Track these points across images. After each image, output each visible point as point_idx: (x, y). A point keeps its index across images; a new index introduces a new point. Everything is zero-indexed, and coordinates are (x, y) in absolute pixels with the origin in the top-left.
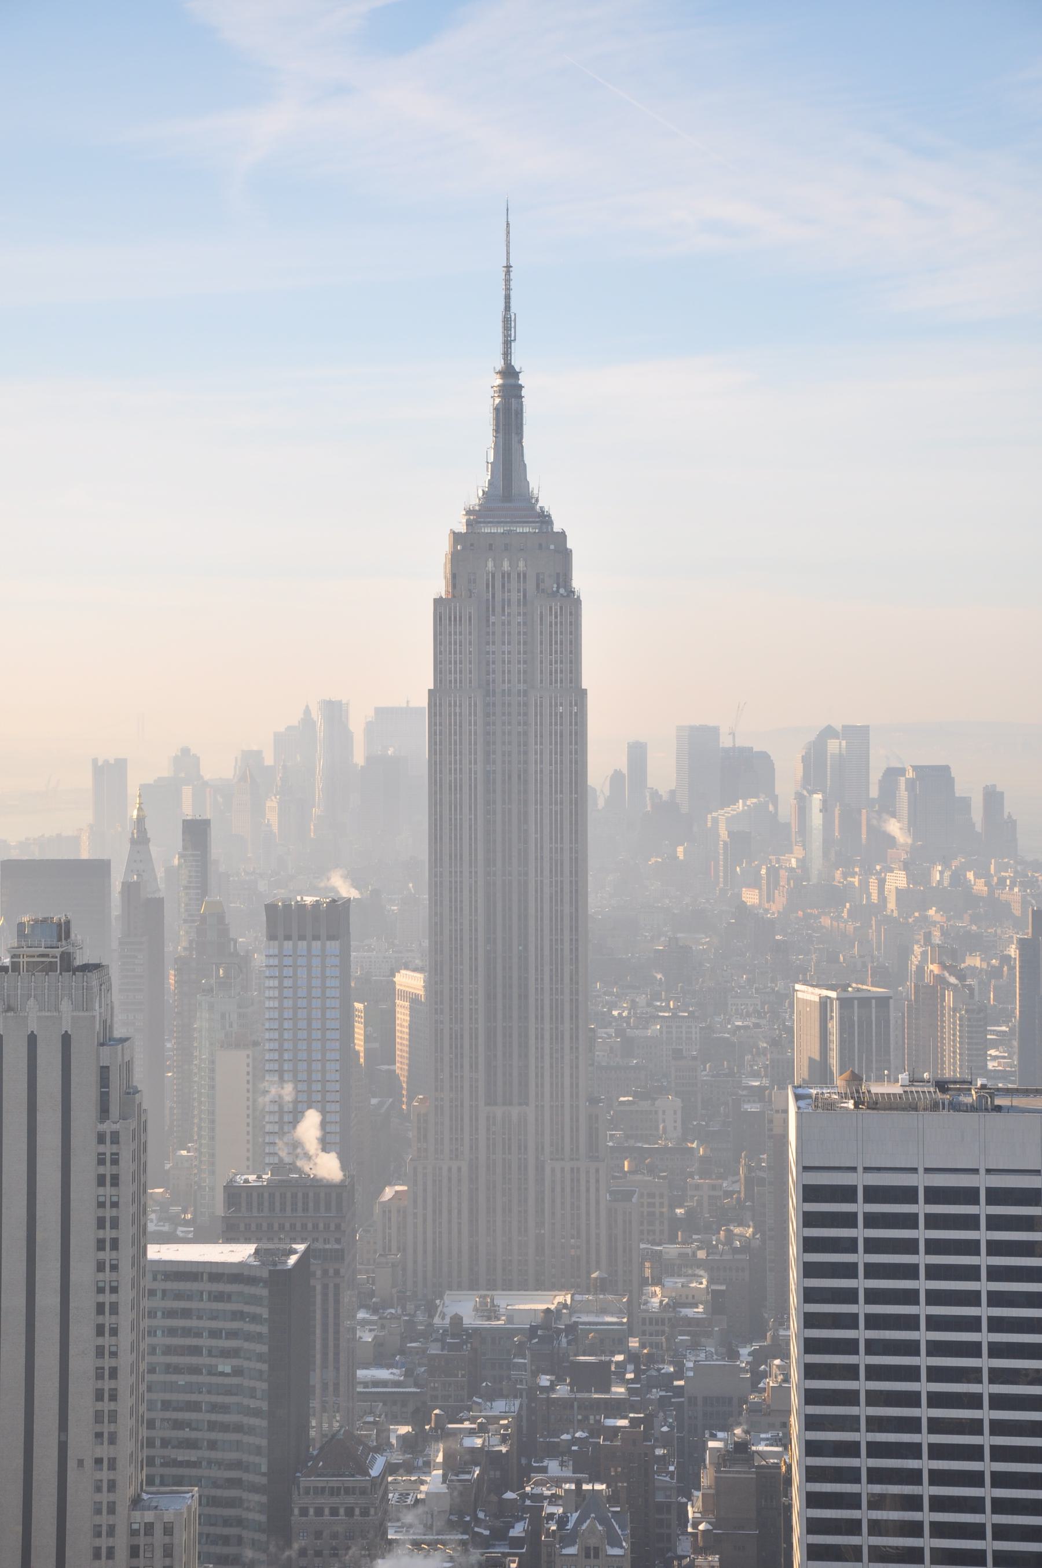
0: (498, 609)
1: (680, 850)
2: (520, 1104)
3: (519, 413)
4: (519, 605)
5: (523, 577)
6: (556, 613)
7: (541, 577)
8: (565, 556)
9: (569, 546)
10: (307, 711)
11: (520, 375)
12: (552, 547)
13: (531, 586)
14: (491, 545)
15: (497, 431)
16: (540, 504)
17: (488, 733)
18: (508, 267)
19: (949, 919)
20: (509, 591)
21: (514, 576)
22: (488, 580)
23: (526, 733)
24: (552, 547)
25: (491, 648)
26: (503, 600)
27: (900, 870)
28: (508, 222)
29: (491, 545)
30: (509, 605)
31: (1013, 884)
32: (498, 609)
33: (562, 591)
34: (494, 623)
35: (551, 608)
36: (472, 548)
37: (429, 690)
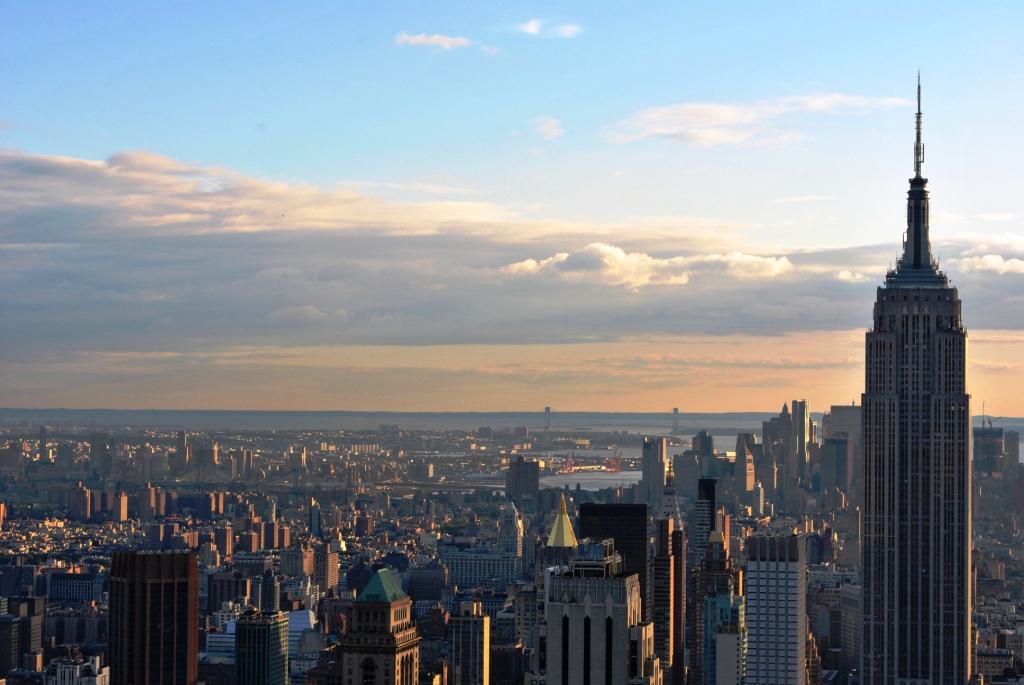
0: (910, 340)
2: (923, 678)
4: (924, 337)
5: (927, 318)
10: (785, 408)
11: (927, 185)
12: (948, 298)
13: (933, 325)
15: (909, 221)
18: (919, 115)
20: (918, 328)
23: (928, 424)
24: (948, 298)
25: (905, 367)
26: (914, 333)
30: (918, 337)
32: (910, 340)
33: (954, 328)
37: (863, 395)
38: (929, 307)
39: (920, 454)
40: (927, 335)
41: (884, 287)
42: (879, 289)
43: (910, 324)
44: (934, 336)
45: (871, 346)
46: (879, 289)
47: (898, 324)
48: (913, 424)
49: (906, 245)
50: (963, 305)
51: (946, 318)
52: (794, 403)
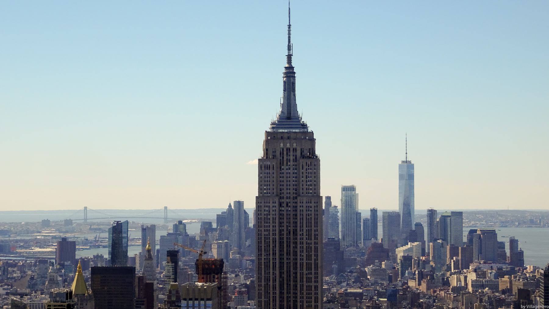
0: (285, 163)
1: (383, 263)
3: (294, 84)
4: (293, 161)
5: (295, 150)
6: (309, 165)
7: (303, 150)
8: (312, 141)
9: (314, 138)
10: (230, 206)
11: (294, 68)
13: (298, 153)
14: (282, 137)
15: (284, 91)
16: (302, 120)
17: (281, 215)
18: (289, 26)
19: (493, 292)
20: (290, 156)
21: (291, 150)
22: (281, 151)
24: (307, 138)
26: (287, 159)
27: (473, 272)
28: (289, 8)
29: (282, 137)
30: (290, 161)
31: (520, 277)
32: (285, 163)
34: (283, 169)
35: (306, 163)
36: (274, 138)
37: (256, 197)
38: (296, 143)
39: (292, 233)
40: (295, 160)
41: (269, 130)
42: (266, 132)
43: (285, 153)
44: (299, 160)
45: (261, 167)
46: (266, 132)
47: (278, 154)
48: (287, 215)
49: (283, 106)
50: (317, 142)
51: (306, 150)
52: (235, 202)
